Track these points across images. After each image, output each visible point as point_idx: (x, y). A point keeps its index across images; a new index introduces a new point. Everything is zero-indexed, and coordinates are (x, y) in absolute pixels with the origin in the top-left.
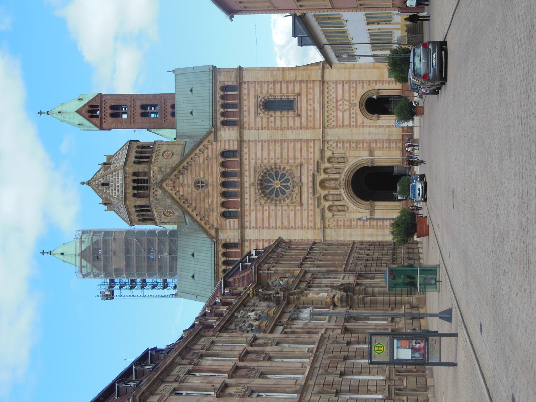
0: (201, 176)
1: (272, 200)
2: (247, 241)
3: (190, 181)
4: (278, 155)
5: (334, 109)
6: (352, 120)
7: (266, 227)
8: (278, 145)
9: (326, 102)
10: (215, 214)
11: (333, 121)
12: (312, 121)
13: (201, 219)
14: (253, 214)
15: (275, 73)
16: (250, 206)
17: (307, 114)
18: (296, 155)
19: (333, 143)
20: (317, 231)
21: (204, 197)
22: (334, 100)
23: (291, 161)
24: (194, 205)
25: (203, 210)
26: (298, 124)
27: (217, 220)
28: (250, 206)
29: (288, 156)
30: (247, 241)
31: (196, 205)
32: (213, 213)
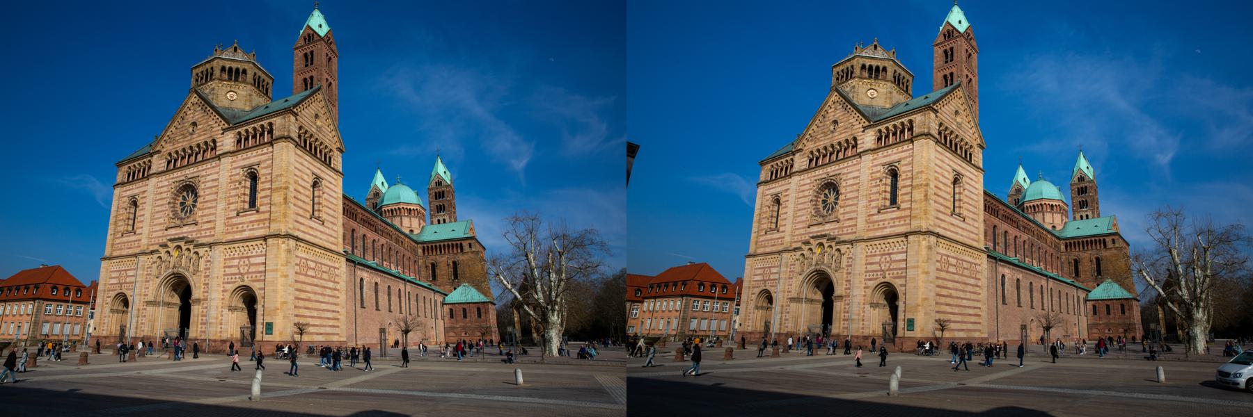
1: (816, 196)
3: (837, 115)
4: (849, 196)
6: (871, 274)
8: (855, 194)
9: (889, 240)
10: (812, 146)
12: (876, 227)
15: (919, 175)
17: (881, 221)
18: (846, 215)
20: (789, 245)
22: (891, 251)
23: (842, 211)
24: (820, 125)
28: (814, 176)
29: (847, 206)
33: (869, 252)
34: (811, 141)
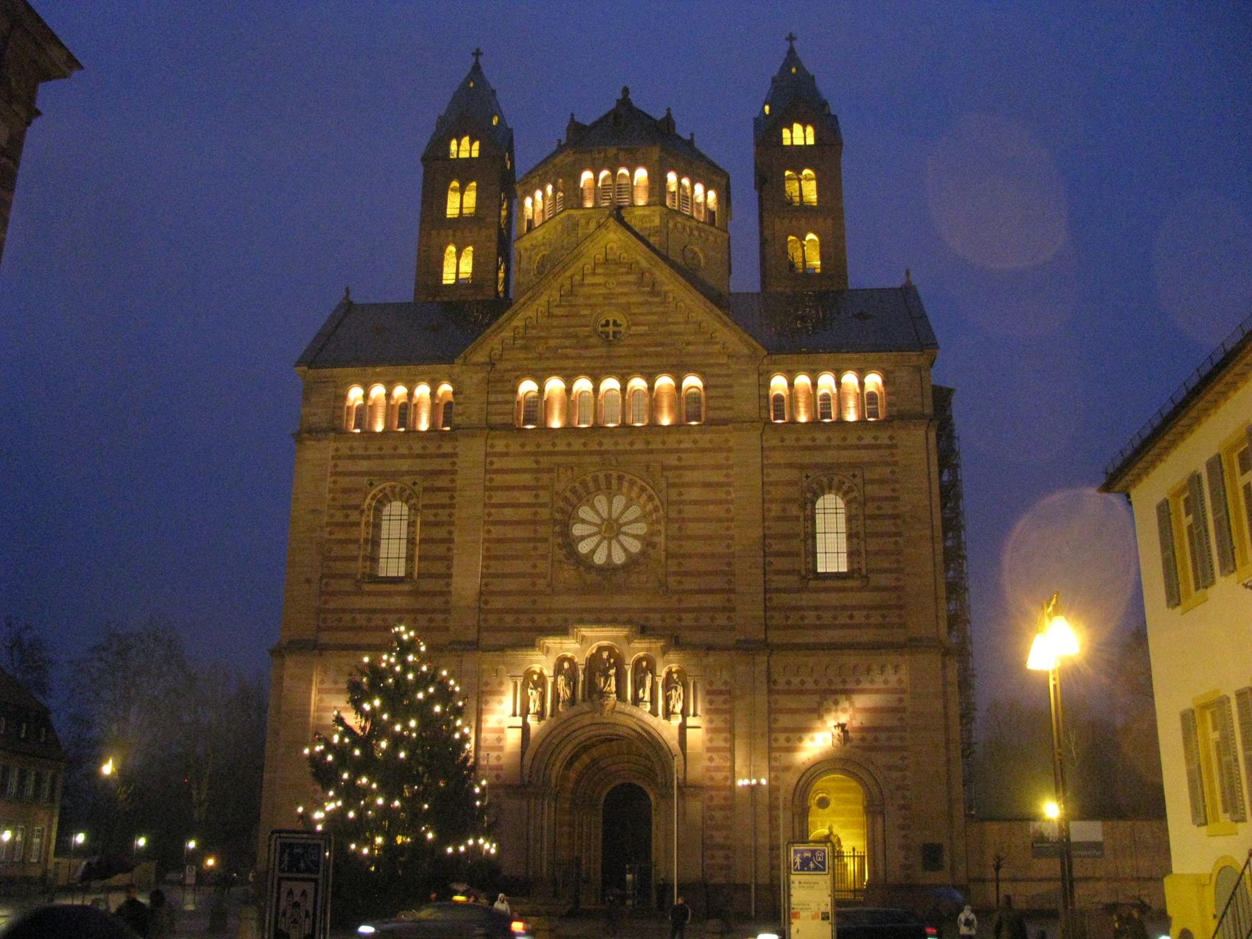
0: (633, 328)
2: (454, 448)
5: (824, 685)
7: (490, 497)
11: (789, 683)
13: (517, 327)
14: (528, 463)
16: (550, 454)
19: (726, 683)
21: (576, 336)
24: (556, 311)
25: (543, 334)
26: (778, 581)
27: (515, 370)
28: (550, 454)
30: (454, 448)
31: (557, 316)
32: (532, 359)
33: (782, 680)
34: (525, 348)
